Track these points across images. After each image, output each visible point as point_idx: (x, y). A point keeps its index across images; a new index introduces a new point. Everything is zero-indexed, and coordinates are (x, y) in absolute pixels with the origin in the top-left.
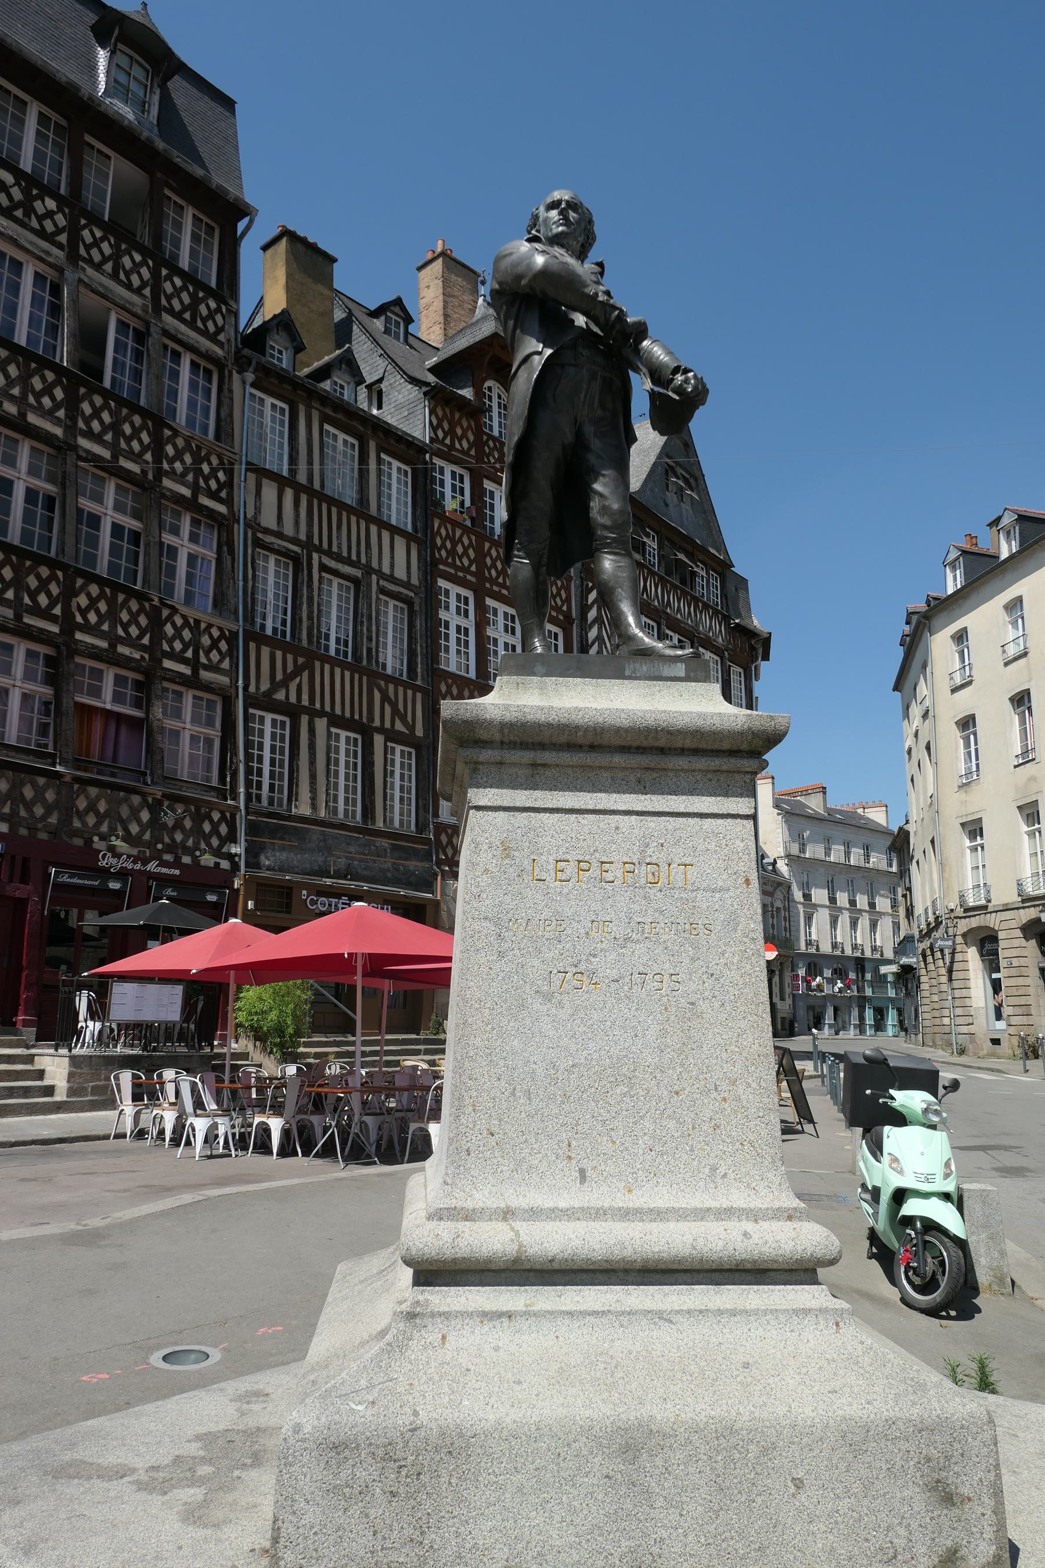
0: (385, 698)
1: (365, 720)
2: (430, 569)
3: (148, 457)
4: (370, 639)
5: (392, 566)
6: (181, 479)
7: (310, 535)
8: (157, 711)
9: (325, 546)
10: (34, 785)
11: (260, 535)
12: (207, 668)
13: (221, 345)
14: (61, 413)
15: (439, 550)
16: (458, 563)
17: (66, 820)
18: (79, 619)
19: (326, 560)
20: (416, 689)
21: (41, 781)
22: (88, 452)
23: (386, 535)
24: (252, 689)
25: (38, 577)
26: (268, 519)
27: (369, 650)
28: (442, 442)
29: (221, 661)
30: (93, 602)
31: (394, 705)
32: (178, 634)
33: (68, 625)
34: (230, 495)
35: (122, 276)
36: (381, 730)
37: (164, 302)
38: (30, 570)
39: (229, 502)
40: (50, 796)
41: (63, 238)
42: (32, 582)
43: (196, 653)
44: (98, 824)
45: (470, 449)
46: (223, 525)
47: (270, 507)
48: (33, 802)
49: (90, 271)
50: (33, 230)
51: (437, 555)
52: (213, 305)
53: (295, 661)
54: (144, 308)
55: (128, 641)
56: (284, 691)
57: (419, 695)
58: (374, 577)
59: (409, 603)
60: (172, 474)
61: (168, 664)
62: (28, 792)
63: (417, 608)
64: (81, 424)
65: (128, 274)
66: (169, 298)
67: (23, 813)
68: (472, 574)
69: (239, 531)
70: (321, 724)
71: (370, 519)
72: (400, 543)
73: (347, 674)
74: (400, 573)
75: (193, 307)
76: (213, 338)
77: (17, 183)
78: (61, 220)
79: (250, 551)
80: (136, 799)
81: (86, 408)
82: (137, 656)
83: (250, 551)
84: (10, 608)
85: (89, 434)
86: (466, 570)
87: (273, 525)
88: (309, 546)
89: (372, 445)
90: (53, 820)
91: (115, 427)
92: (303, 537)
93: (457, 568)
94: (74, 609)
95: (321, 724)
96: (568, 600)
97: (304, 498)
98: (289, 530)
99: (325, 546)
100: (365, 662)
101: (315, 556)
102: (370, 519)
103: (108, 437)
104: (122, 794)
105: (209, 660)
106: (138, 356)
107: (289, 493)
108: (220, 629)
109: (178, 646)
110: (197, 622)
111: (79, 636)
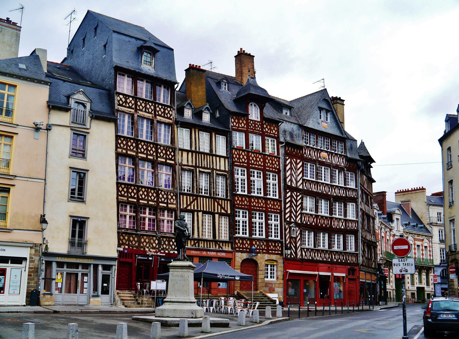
0: (218, 204)
2: (232, 165)
3: (155, 154)
4: (214, 188)
5: (220, 167)
7: (196, 163)
8: (159, 216)
9: (200, 165)
12: (170, 204)
13: (171, 119)
14: (135, 149)
15: (235, 158)
16: (241, 161)
17: (139, 244)
18: (140, 197)
19: (201, 170)
20: (227, 200)
21: (134, 236)
22: (141, 157)
23: (218, 158)
24: (182, 207)
25: (131, 189)
26: (185, 162)
27: (214, 192)
28: (235, 126)
30: (143, 192)
31: (221, 206)
32: (163, 197)
33: (138, 199)
34: (175, 158)
35: (147, 111)
36: (217, 213)
39: (174, 160)
40: (136, 239)
41: (134, 107)
42: (130, 191)
43: (167, 201)
44: (146, 245)
45: (244, 126)
46: (172, 167)
47: (185, 159)
49: (140, 112)
50: (128, 107)
52: (169, 109)
53: (193, 198)
54: (152, 117)
57: (229, 202)
58: (215, 171)
59: (225, 176)
61: (161, 204)
62: (131, 239)
63: (228, 177)
64: (139, 151)
65: (148, 109)
66: (158, 112)
67: (130, 243)
68: (246, 163)
69: (177, 167)
70: (200, 214)
71: (213, 155)
72: (222, 160)
73: (207, 199)
74: (222, 168)
75: (164, 112)
76: (169, 118)
77: (124, 97)
78: (133, 102)
80: (155, 238)
81: (140, 146)
82: (153, 203)
85: (141, 153)
89: (213, 134)
90: (137, 244)
92: (194, 164)
95: (200, 214)
96: (279, 165)
97: (194, 154)
99: (200, 165)
101: (198, 169)
102: (213, 155)
106: (151, 129)
107: (190, 154)
108: (173, 193)
109: (163, 199)
110: (167, 193)
111: (141, 201)
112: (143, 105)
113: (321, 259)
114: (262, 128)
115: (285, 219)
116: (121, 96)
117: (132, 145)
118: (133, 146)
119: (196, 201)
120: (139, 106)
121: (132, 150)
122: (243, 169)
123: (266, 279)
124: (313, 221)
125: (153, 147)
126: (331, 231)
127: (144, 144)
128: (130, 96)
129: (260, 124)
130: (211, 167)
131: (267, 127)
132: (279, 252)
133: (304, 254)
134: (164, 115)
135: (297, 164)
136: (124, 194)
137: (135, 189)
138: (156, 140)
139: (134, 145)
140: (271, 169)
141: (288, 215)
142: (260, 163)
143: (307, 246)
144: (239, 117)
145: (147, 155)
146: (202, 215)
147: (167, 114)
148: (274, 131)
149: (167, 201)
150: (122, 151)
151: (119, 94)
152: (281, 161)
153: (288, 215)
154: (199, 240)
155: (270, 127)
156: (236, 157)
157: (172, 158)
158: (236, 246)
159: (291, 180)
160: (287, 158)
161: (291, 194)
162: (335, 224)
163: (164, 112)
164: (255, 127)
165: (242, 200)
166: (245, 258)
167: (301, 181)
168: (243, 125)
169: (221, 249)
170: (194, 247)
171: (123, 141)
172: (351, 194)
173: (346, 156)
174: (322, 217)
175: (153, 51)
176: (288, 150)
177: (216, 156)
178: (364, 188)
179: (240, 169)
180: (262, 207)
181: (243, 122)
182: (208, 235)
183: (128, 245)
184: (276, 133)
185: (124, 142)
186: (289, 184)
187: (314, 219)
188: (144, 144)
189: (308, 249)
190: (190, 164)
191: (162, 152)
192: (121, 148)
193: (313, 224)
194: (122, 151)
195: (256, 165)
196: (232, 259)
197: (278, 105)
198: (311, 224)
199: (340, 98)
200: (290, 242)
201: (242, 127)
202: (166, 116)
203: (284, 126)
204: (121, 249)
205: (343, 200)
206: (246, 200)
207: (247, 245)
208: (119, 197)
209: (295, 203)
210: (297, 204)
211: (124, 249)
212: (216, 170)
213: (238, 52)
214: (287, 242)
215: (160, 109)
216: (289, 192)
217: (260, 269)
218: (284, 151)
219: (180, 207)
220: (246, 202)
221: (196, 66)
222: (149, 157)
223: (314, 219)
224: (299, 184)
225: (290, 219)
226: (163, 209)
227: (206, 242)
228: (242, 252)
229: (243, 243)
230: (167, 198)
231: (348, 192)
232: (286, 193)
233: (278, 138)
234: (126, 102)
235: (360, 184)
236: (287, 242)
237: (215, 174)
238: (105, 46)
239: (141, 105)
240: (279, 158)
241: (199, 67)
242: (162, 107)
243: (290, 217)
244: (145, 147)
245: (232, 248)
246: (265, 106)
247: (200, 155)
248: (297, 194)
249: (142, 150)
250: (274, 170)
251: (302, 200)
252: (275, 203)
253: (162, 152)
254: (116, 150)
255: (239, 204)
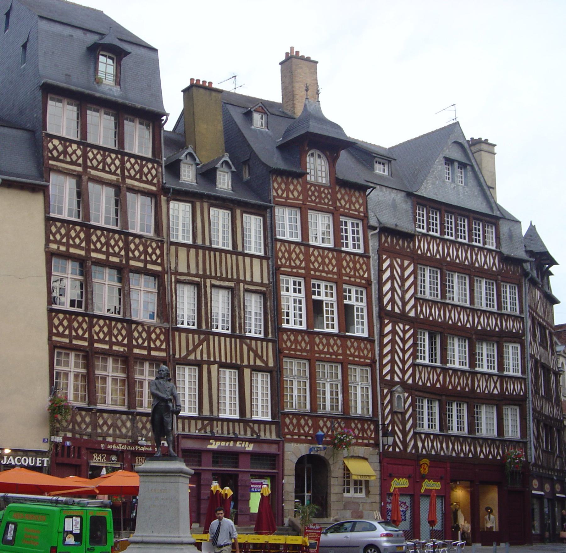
0: (250, 349)
1: (239, 362)
2: (276, 271)
3: (123, 253)
5: (252, 276)
6: (138, 259)
9: (213, 274)
10: (81, 415)
11: (178, 277)
13: (154, 185)
15: (281, 259)
18: (96, 337)
20: (268, 341)
21: (84, 413)
24: (177, 356)
25: (78, 322)
26: (182, 268)
27: (240, 324)
28: (281, 197)
29: (161, 345)
30: (101, 328)
31: (255, 353)
33: (91, 341)
34: (162, 260)
35: (107, 169)
36: (248, 366)
37: (127, 174)
38: (75, 319)
40: (88, 419)
41: (80, 161)
42: (76, 325)
43: (149, 343)
45: (299, 196)
47: (183, 262)
48: (81, 423)
49: (93, 172)
51: (279, 263)
53: (199, 338)
55: (118, 344)
56: (194, 354)
57: (270, 344)
58: (242, 284)
59: (263, 294)
60: (134, 258)
61: (136, 351)
63: (268, 296)
64: (92, 247)
67: (77, 428)
70: (214, 368)
71: (238, 254)
72: (256, 262)
73: (228, 339)
74: (257, 279)
75: (141, 171)
76: (151, 183)
77: (61, 143)
78: (79, 152)
79: (173, 287)
81: (94, 238)
82: (122, 349)
83: (173, 287)
84: (67, 338)
85: (96, 250)
86: (299, 267)
87: (185, 271)
88: (205, 276)
89: (238, 212)
91: (107, 244)
92: (201, 272)
93: (293, 268)
94: (93, 333)
95: (214, 368)
96: (368, 269)
97: (200, 251)
98: (193, 271)
99: (213, 274)
100: (238, 332)
101: (208, 281)
102: (238, 254)
103: (104, 249)
104: (118, 415)
105: (155, 345)
107: (193, 251)
108: (160, 329)
109: (140, 341)
110: (149, 328)
111: (96, 345)
112: (99, 157)
113: (454, 454)
114: (335, 200)
115: (382, 377)
116: (56, 142)
117: (78, 236)
118: (80, 238)
119: (205, 343)
120: (91, 161)
121: (78, 247)
122: (298, 280)
123: (346, 495)
124: (438, 380)
125: (120, 238)
126: (473, 400)
127: (103, 234)
128: (72, 142)
129: (329, 193)
130: (235, 277)
131: (343, 197)
132: (371, 441)
133: (420, 445)
134: (141, 177)
135: (403, 269)
136: (64, 331)
137: (84, 320)
138: (125, 224)
139: (82, 235)
140: (353, 279)
141: (388, 368)
142: (331, 267)
143: (426, 429)
144: (287, 179)
145: (108, 254)
146: (218, 371)
147: (146, 175)
148: (357, 206)
149: (149, 343)
150: (58, 248)
151: (53, 137)
152: (373, 262)
153: (388, 368)
154: (212, 420)
155: (350, 197)
156: (283, 256)
157: (157, 259)
158: (286, 430)
159: (392, 300)
160: (384, 257)
161: (394, 327)
162: (481, 386)
163: (141, 171)
164: (319, 196)
165: (296, 340)
166: (304, 453)
167: (412, 302)
168: (296, 194)
169: (255, 436)
170: (202, 433)
171: (60, 228)
172: (511, 326)
173: (500, 252)
174: (455, 371)
175: (117, 55)
176: (386, 241)
177: (245, 255)
178: (537, 313)
179: (291, 280)
180: (336, 354)
181: (295, 188)
182: (229, 412)
183: (73, 431)
184: (362, 209)
185: (63, 231)
186: (389, 308)
187: (438, 376)
188: (103, 234)
189: (428, 435)
190: (193, 271)
191: (137, 248)
192: (55, 241)
193: (438, 385)
194: (58, 248)
195: (323, 271)
196: (278, 454)
197: (366, 154)
198: (433, 385)
199: (486, 140)
200: (393, 422)
201: (294, 199)
202: (144, 178)
203: (376, 196)
204: (59, 439)
205: (496, 339)
206: (303, 339)
207: (307, 429)
208: (54, 338)
209: (402, 346)
210: (404, 346)
211: (65, 439)
212: (245, 282)
213: (287, 54)
214: (387, 422)
215: (133, 166)
216: (388, 324)
217: (333, 475)
218: (377, 244)
219: (174, 355)
220: (303, 344)
221: (204, 82)
222: (112, 259)
223: (438, 376)
224: (408, 308)
225: (392, 377)
226: (141, 359)
227: (225, 423)
228: (298, 441)
229: (299, 425)
230: (149, 339)
231: (506, 322)
232: (382, 326)
233: (365, 218)
234: (65, 152)
235: (530, 306)
236: (387, 422)
237: (242, 289)
238: (24, 46)
239: (95, 157)
240: (369, 257)
241: (210, 83)
242: (136, 162)
243: (392, 372)
244: (103, 240)
245: (278, 435)
246: (337, 157)
247: (212, 253)
248: (404, 328)
249: (99, 245)
250: (358, 280)
251: (415, 340)
252: (362, 345)
253: (137, 248)
254: (47, 245)
255: (290, 349)
